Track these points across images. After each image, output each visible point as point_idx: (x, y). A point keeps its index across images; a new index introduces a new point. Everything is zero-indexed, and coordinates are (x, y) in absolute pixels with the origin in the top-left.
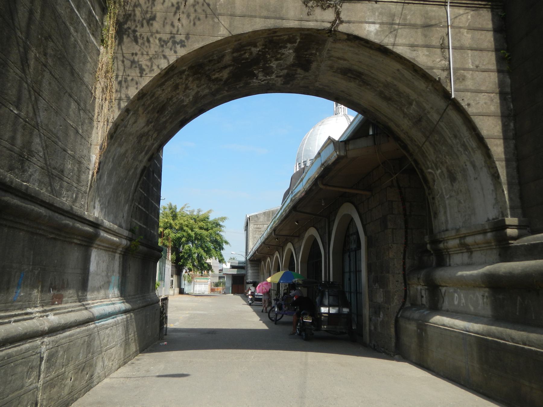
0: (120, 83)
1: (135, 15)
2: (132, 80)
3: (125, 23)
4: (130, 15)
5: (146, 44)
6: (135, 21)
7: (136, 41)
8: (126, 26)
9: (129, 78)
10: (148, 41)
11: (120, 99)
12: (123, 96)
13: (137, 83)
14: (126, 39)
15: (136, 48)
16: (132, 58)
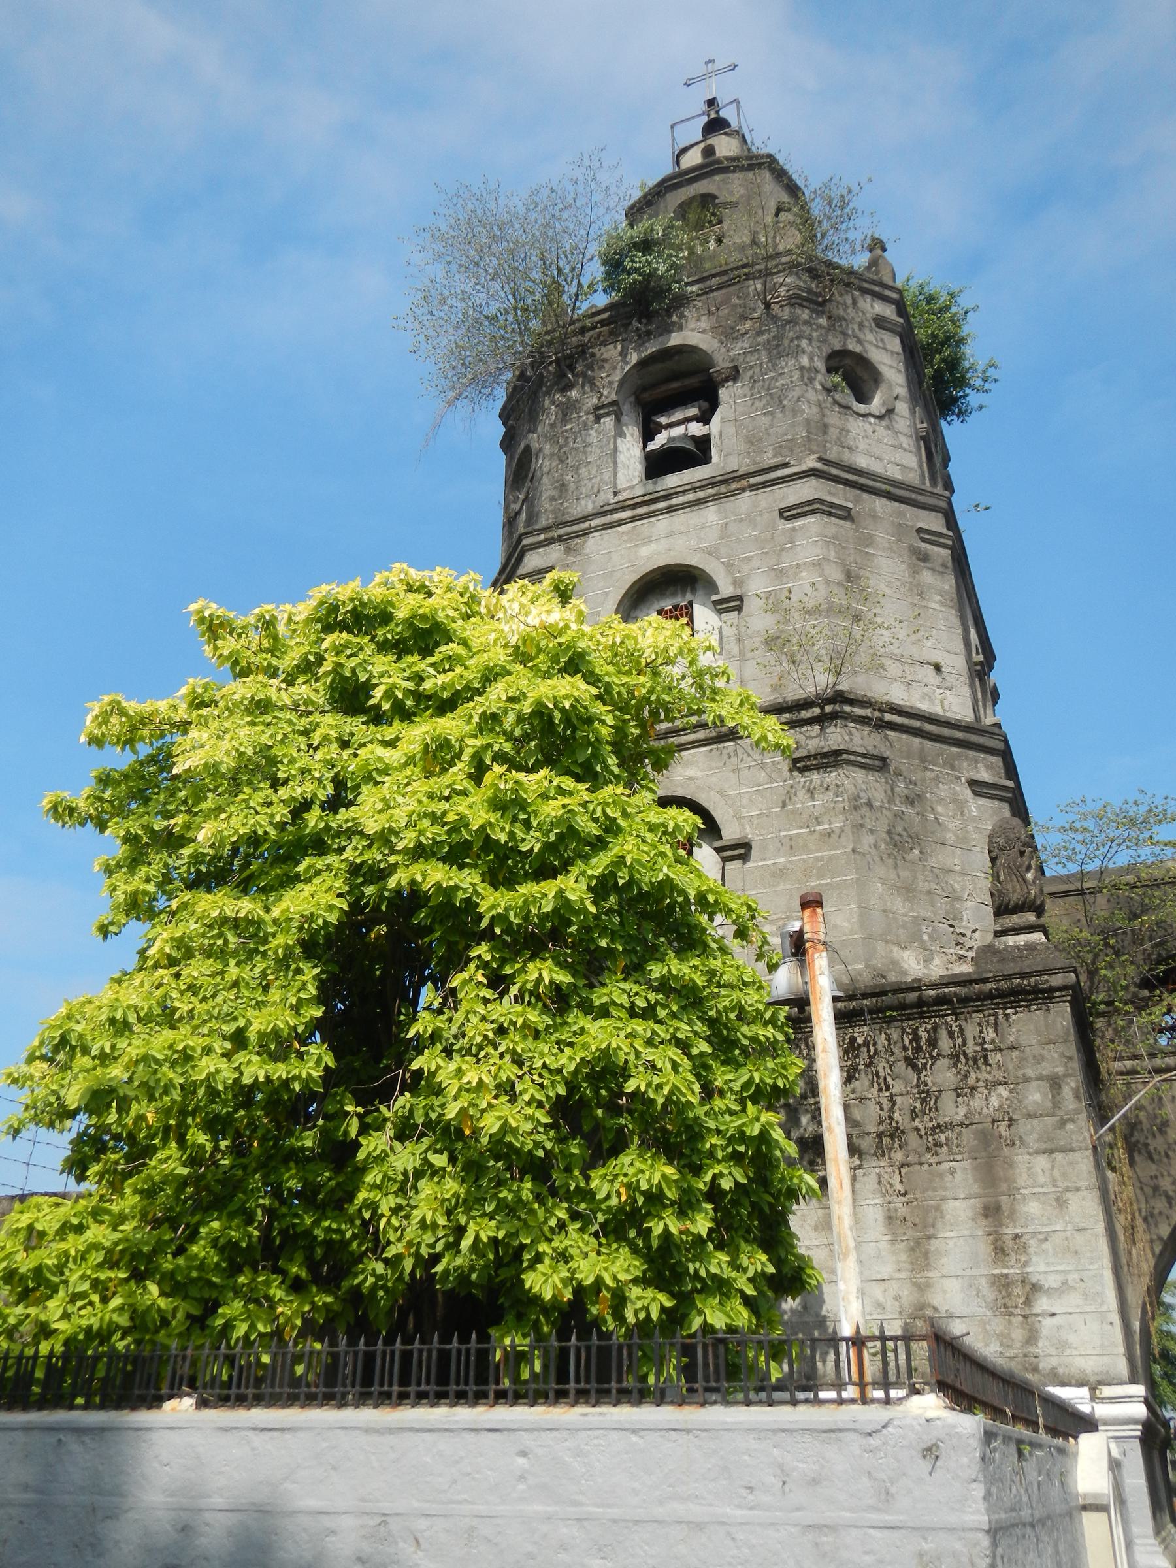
0: (1145, 1220)
1: (1141, 1123)
2: (1160, 1213)
3: (1132, 1135)
4: (1135, 1124)
5: (1165, 1160)
6: (1142, 1130)
7: (1151, 1158)
8: (1133, 1140)
9: (1156, 1211)
10: (1167, 1156)
11: (1152, 1241)
12: (1155, 1237)
13: (1168, 1218)
14: (1137, 1158)
15: (1153, 1169)
16: (1152, 1184)
